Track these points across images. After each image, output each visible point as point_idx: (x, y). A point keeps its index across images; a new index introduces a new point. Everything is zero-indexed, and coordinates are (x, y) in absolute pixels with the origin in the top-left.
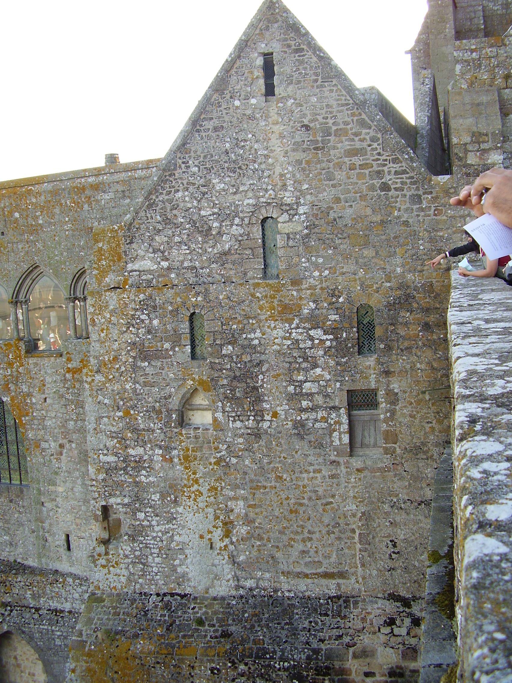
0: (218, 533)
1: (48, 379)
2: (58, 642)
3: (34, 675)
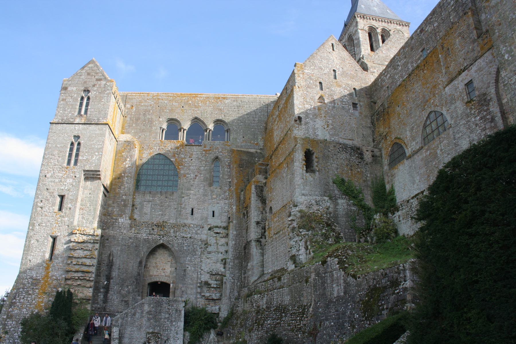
0: (326, 126)
1: (194, 153)
2: (185, 248)
3: (165, 269)
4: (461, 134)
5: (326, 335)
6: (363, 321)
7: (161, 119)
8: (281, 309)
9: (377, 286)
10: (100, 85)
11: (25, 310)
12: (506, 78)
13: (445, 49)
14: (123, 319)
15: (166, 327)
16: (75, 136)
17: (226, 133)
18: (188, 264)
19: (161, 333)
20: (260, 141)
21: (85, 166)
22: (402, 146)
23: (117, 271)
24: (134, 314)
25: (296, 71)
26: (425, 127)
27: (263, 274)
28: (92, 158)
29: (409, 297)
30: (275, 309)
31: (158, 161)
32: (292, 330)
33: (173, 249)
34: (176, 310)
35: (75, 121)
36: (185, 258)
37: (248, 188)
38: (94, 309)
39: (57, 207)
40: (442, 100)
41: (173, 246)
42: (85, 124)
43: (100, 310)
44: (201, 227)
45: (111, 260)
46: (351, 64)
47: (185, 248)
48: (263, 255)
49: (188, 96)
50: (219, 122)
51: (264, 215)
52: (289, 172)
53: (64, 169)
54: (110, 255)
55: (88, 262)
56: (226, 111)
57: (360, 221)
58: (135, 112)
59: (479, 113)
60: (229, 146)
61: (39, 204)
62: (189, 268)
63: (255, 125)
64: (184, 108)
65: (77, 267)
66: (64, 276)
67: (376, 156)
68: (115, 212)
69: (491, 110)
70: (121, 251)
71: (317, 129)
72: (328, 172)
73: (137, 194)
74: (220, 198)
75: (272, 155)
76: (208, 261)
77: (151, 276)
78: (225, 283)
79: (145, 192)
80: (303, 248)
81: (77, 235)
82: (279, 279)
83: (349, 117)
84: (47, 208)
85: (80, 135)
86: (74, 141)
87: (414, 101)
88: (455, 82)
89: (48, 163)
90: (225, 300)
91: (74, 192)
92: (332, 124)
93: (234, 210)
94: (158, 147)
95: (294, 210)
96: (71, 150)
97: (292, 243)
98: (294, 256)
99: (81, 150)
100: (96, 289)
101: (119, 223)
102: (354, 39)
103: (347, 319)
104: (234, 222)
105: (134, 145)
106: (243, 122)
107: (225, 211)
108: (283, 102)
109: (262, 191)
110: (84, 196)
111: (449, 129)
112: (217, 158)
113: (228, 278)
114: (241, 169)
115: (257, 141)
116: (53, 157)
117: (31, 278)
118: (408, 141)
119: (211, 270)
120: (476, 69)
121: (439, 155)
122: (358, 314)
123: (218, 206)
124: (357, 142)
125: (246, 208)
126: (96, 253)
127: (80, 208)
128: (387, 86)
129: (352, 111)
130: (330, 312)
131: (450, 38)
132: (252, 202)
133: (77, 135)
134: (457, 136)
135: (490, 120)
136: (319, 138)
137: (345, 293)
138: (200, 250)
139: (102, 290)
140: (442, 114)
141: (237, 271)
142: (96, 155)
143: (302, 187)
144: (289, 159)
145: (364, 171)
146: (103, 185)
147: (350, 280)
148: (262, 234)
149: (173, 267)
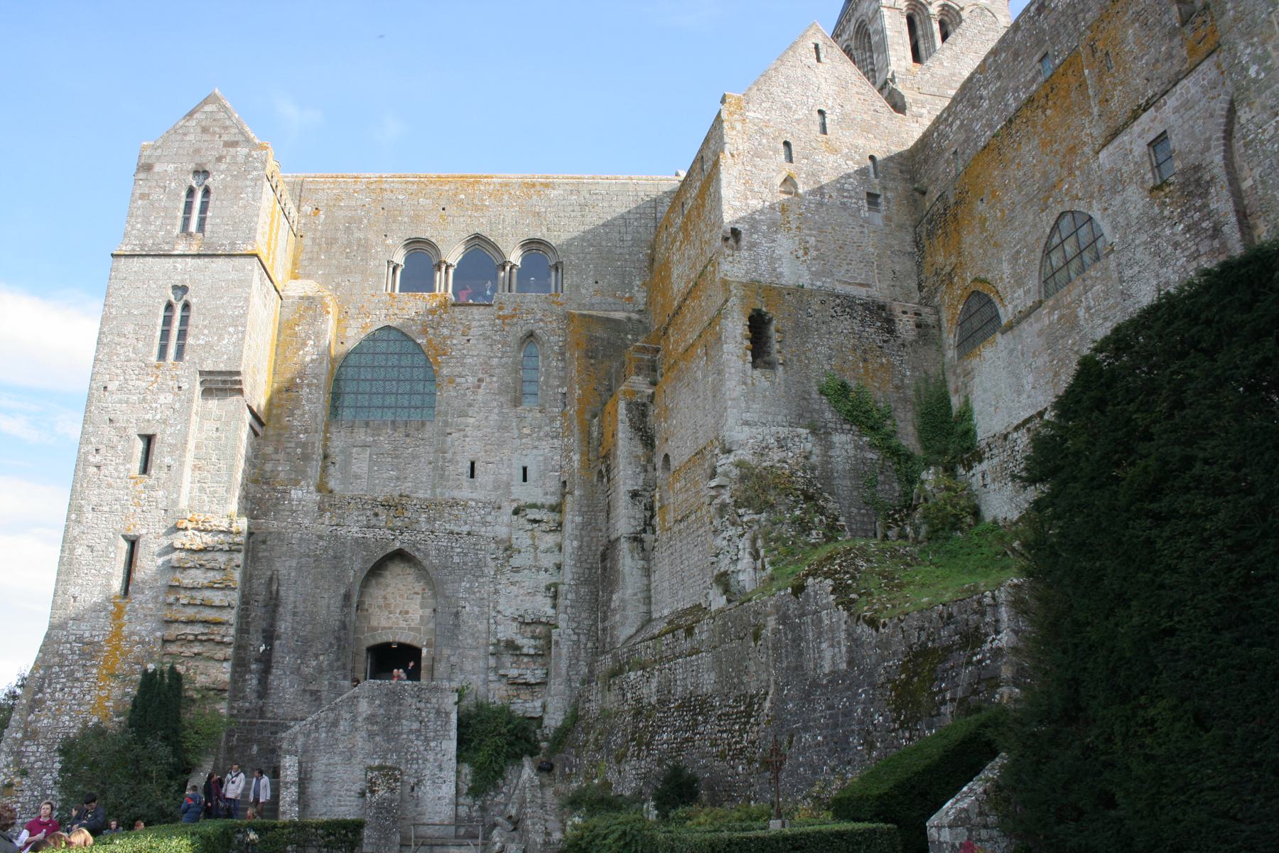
0: (801, 253)
1: (474, 324)
2: (456, 559)
4: (1136, 269)
5: (804, 766)
6: (894, 730)
7: (389, 241)
8: (695, 706)
9: (930, 644)
10: (234, 157)
11: (67, 718)
12: (1251, 126)
13: (1099, 54)
15: (413, 753)
16: (175, 288)
17: (553, 274)
18: (465, 599)
19: (402, 768)
20: (638, 291)
21: (202, 360)
22: (990, 301)
23: (289, 618)
24: (335, 724)
25: (724, 116)
26: (1047, 252)
27: (648, 620)
28: (219, 340)
29: (1006, 672)
30: (679, 706)
31: (385, 344)
32: (722, 756)
33: (426, 563)
34: (438, 712)
35: (174, 250)
36: (456, 585)
37: (608, 407)
38: (235, 712)
39: (136, 465)
40: (1090, 185)
41: (427, 555)
42: (199, 256)
43: (250, 715)
44: (494, 508)
45: (274, 592)
46: (862, 94)
47: (456, 559)
48: (648, 572)
49: (456, 182)
50: (534, 246)
51: (650, 475)
52: (710, 368)
53: (150, 370)
54: (271, 579)
55: (217, 598)
56: (550, 217)
57: (887, 487)
58: (324, 224)
59: (1183, 215)
60: (561, 304)
61: (91, 459)
62: (467, 609)
63: (626, 251)
64: (447, 212)
65: (190, 612)
66: (158, 634)
67: (927, 326)
68: (282, 475)
69: (1213, 206)
70: (299, 569)
71: (780, 259)
72: (807, 366)
73: (333, 429)
74: (542, 434)
75: (669, 324)
76: (514, 589)
77: (374, 629)
78: (557, 642)
79: (354, 422)
80: (747, 556)
81: (189, 533)
82: (689, 631)
83: (858, 229)
84: (111, 468)
85: (188, 284)
86: (172, 298)
87: (1020, 188)
88: (1124, 138)
89: (110, 354)
90: (557, 686)
91: (179, 427)
92: (816, 246)
93: (576, 465)
94: (384, 311)
95: (724, 461)
96: (167, 321)
97: (720, 542)
98: (725, 574)
99: (191, 321)
100: (240, 664)
101: (291, 500)
102: (871, 31)
103: (856, 728)
104: (577, 493)
105: (324, 306)
106: (595, 243)
107: (553, 466)
108: (694, 193)
109: (644, 415)
110: (204, 435)
111: (1107, 255)
112: (531, 335)
113: (564, 632)
114: (593, 361)
115: (630, 291)
116: (123, 339)
117: (80, 639)
118: (1005, 288)
119: (522, 612)
120: (1176, 104)
121: (1082, 322)
122: (881, 715)
123: (536, 456)
124: (879, 291)
125: (604, 457)
126: (237, 575)
127: (195, 466)
128: (953, 149)
129: (867, 215)
130: (815, 710)
131: (1112, 26)
132: (620, 443)
133: (180, 285)
134: (1128, 273)
135: (1210, 232)
136: (783, 282)
137: (850, 663)
138: (494, 564)
139: (253, 667)
140: (1090, 218)
141: (583, 615)
142: (229, 333)
143: (743, 405)
144: (711, 337)
145: (897, 363)
146: (250, 408)
147: (863, 631)
148: (645, 524)
149: (426, 607)
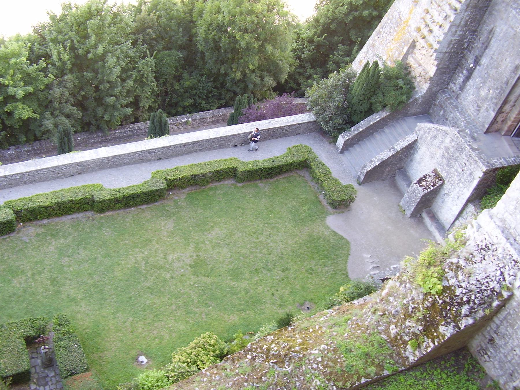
14: (425, 132)
24: (435, 137)
139: (465, 72)
